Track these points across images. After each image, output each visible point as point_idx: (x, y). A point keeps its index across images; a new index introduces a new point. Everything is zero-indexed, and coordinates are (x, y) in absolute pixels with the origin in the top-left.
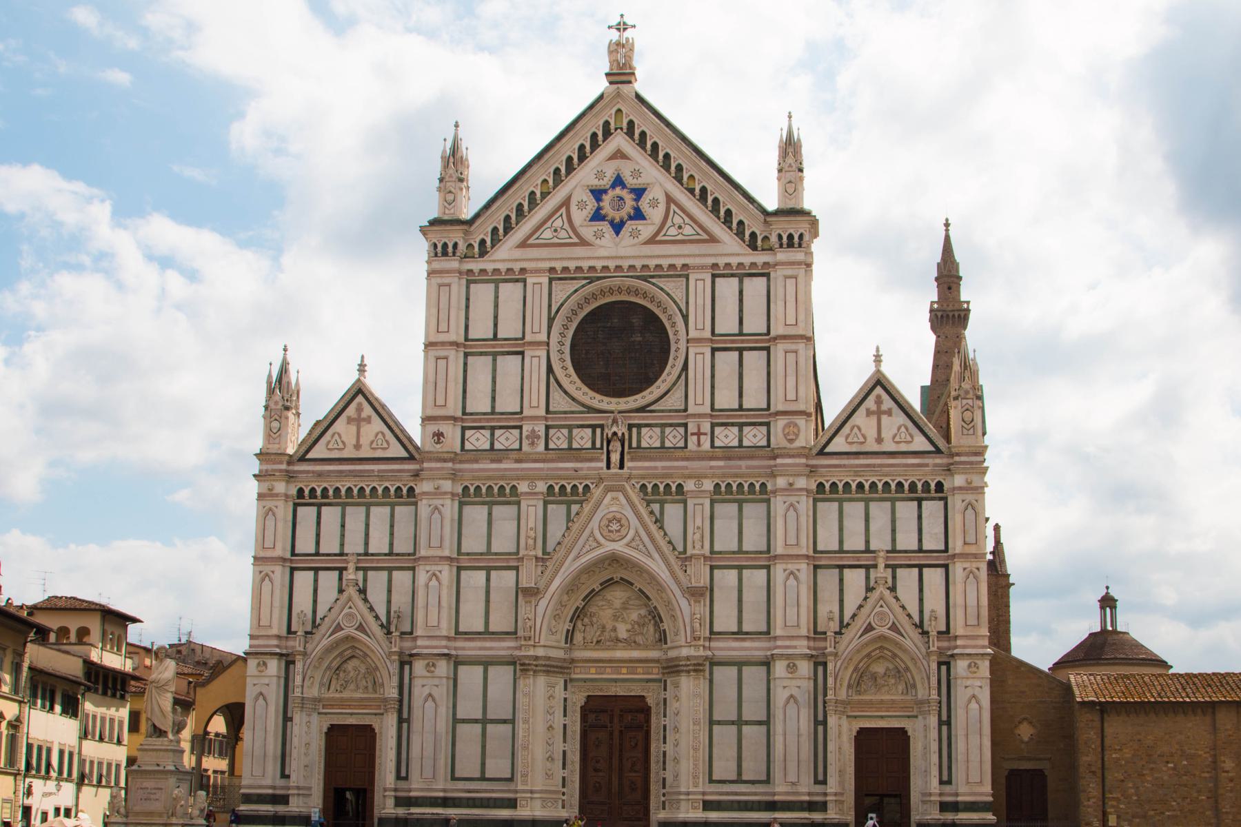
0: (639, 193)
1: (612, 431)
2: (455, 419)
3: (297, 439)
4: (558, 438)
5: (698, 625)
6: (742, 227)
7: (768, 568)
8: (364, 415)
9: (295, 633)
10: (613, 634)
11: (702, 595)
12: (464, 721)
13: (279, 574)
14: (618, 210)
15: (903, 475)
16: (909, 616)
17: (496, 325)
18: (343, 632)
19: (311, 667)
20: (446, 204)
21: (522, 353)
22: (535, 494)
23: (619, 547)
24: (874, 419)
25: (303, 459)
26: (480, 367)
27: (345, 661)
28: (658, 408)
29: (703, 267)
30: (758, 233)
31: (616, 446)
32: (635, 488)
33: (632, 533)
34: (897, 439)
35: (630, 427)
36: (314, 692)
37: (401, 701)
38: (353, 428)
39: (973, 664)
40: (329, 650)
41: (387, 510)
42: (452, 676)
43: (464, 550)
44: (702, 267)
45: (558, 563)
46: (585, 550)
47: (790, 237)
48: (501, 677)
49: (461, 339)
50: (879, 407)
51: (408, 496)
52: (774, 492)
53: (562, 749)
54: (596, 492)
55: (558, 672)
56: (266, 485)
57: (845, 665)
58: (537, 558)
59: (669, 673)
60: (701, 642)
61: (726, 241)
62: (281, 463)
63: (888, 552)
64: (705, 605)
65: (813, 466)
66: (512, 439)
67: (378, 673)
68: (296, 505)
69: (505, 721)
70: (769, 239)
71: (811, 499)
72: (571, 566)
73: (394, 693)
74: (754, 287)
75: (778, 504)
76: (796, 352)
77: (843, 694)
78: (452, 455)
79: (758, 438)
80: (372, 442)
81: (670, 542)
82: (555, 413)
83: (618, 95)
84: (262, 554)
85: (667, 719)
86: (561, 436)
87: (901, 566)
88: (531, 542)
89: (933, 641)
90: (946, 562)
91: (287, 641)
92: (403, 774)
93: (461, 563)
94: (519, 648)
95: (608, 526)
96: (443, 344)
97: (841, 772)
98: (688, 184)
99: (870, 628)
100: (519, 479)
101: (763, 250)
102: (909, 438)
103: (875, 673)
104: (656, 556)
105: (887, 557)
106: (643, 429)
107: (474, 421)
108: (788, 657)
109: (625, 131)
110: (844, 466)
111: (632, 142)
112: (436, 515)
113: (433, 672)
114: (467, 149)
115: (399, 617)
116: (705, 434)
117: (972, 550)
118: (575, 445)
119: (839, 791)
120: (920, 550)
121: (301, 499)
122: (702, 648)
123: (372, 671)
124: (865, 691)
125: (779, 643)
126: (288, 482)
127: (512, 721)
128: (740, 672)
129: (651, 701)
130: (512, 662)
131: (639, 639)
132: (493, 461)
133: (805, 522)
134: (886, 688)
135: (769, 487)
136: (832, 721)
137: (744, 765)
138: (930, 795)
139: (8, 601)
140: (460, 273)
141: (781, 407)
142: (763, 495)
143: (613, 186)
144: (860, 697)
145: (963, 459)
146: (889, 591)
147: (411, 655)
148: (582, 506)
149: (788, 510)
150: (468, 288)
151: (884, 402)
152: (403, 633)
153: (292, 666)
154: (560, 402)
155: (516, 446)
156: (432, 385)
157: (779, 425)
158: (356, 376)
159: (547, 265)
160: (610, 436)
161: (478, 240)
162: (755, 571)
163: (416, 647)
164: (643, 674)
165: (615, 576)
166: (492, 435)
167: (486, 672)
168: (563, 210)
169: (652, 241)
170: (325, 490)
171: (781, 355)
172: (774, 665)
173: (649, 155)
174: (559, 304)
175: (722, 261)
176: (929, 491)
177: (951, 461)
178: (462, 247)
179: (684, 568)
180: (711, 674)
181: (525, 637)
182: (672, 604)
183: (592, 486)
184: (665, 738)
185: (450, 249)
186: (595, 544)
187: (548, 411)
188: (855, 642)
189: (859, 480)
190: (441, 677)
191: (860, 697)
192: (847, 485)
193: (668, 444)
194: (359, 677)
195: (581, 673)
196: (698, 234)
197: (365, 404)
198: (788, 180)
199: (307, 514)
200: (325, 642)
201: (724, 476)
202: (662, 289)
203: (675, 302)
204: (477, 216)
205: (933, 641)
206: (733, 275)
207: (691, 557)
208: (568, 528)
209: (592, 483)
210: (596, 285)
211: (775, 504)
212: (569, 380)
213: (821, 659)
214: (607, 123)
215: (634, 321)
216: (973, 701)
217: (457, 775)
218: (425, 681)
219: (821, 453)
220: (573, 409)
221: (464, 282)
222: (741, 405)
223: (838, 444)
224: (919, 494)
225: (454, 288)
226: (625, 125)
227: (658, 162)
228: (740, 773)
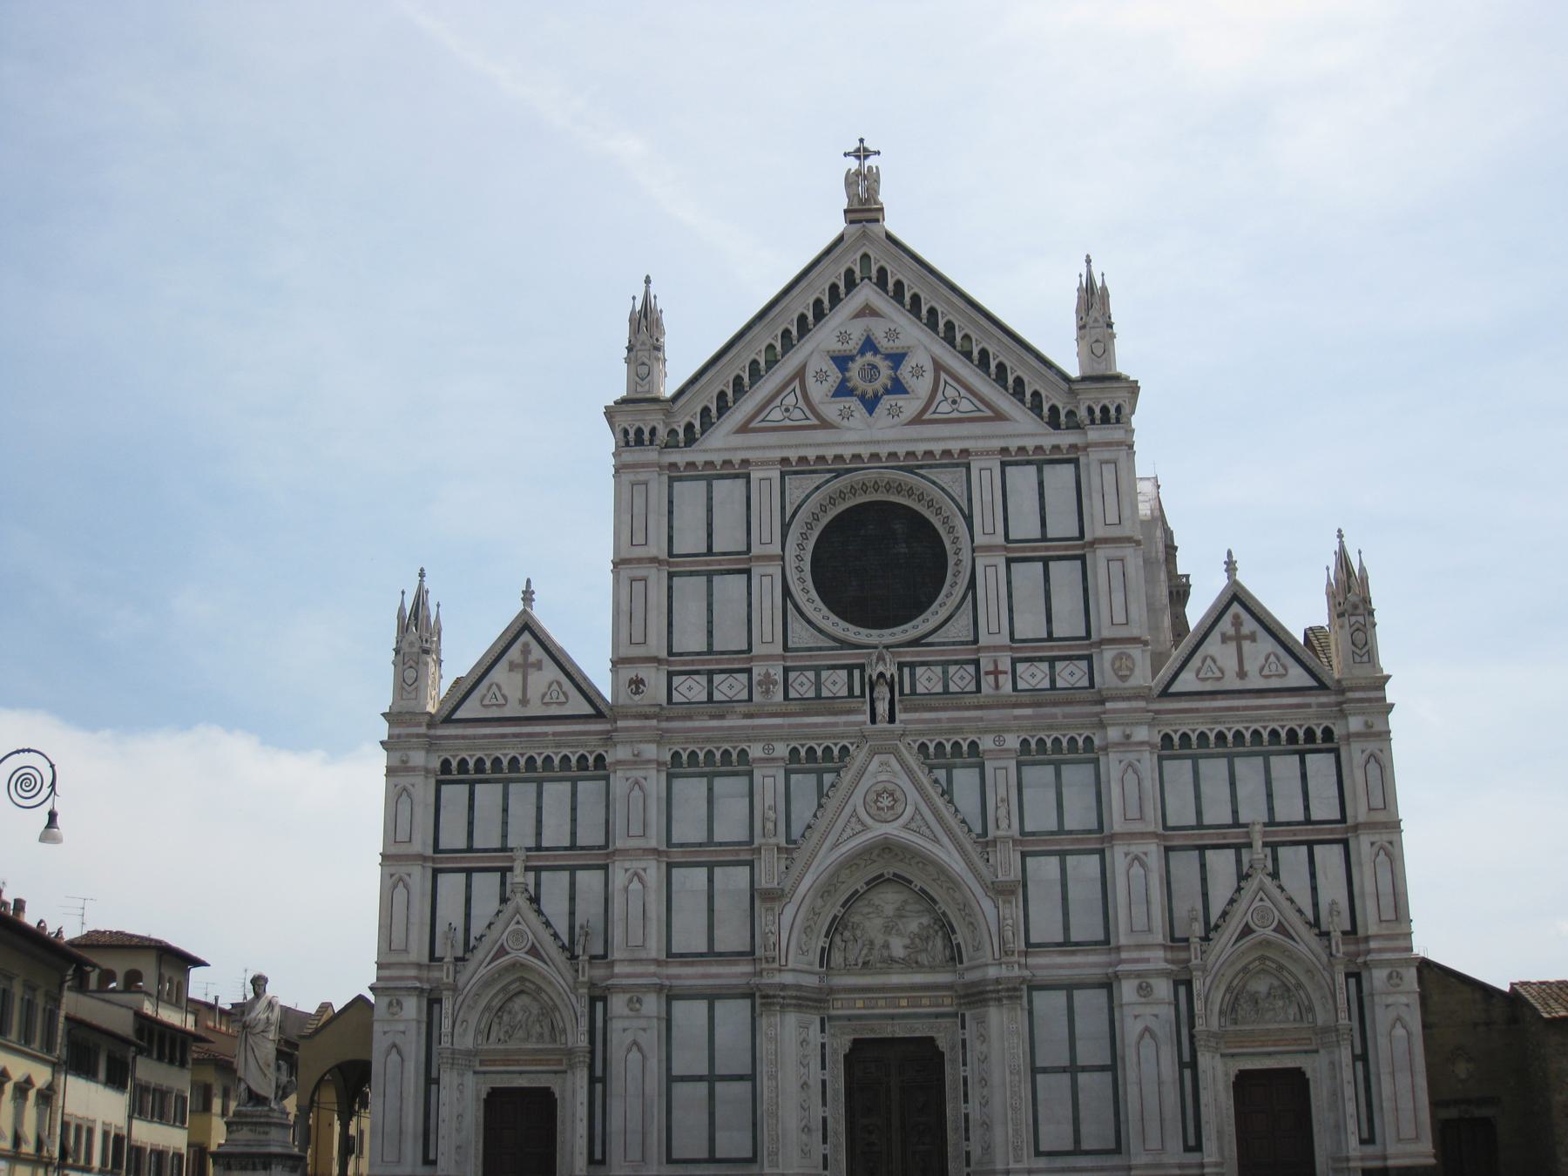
0: (897, 359)
1: (878, 671)
2: (657, 660)
3: (439, 694)
4: (802, 684)
5: (1011, 933)
9: (441, 959)
10: (886, 954)
11: (1013, 892)
12: (683, 1079)
13: (418, 877)
14: (870, 382)
15: (1278, 720)
16: (1300, 911)
17: (710, 536)
18: (507, 957)
19: (465, 1005)
21: (748, 572)
22: (773, 759)
23: (893, 830)
24: (1232, 646)
25: (448, 720)
26: (690, 590)
27: (510, 999)
28: (937, 640)
29: (988, 453)
30: (1060, 406)
31: (883, 691)
32: (911, 748)
34: (1266, 672)
36: (467, 1042)
37: (592, 1052)
39: (1395, 974)
40: (487, 983)
41: (567, 786)
42: (664, 1014)
43: (675, 840)
44: (987, 453)
46: (845, 836)
47: (1105, 410)
48: (733, 1014)
49: (664, 555)
50: (1238, 631)
51: (596, 768)
52: (1105, 749)
53: (820, 1114)
54: (859, 756)
55: (812, 1007)
56: (398, 754)
58: (779, 849)
59: (969, 1003)
60: (1015, 958)
61: (1018, 419)
62: (419, 725)
63: (1265, 825)
64: (1017, 907)
66: (738, 687)
67: (557, 1014)
68: (439, 783)
69: (740, 1078)
70: (1076, 416)
71: (1156, 756)
72: (826, 860)
73: (583, 1041)
74: (1060, 478)
75: (1113, 765)
76: (1122, 560)
78: (657, 709)
80: (544, 696)
82: (797, 650)
84: (394, 850)
85: (968, 1068)
86: (805, 680)
87: (1284, 844)
88: (770, 826)
90: (1345, 836)
91: (429, 971)
92: (598, 1156)
93: (673, 857)
96: (639, 561)
97: (1220, 1134)
98: (962, 346)
99: (1247, 931)
100: (749, 741)
101: (1067, 428)
102: (1281, 671)
103: (1256, 992)
104: (945, 840)
106: (917, 669)
107: (685, 663)
108: (1139, 975)
109: (874, 280)
110: (1197, 710)
111: (885, 295)
112: (637, 792)
113: (638, 1010)
115: (587, 934)
116: (1006, 673)
117: (1380, 817)
118: (825, 693)
120: (1308, 821)
121: (446, 773)
122: (1016, 966)
123: (548, 1012)
126: (428, 751)
127: (752, 1077)
128: (1070, 999)
129: (943, 1045)
131: (923, 958)
132: (712, 717)
133: (1151, 786)
135: (1097, 742)
136: (1204, 1060)
137: (1084, 1129)
138: (1348, 1159)
139: (39, 924)
141: (1106, 634)
142: (1090, 753)
143: (862, 352)
144: (1238, 1028)
145: (1358, 695)
146: (1270, 879)
147: (608, 988)
149: (1125, 771)
150: (670, 487)
151: (1244, 623)
152: (593, 957)
153: (436, 1007)
154: (801, 635)
156: (625, 616)
158: (520, 606)
159: (778, 454)
160: (874, 677)
161: (683, 425)
162: (1084, 858)
163: (612, 976)
164: (930, 1006)
165: (885, 872)
166: (710, 681)
168: (797, 383)
169: (918, 420)
170: (480, 762)
171: (1102, 564)
172: (1120, 987)
173: (908, 311)
174: (795, 506)
175: (1013, 444)
177: (1340, 699)
178: (662, 433)
179: (986, 856)
180: (1030, 1002)
181: (766, 958)
184: (966, 1095)
185: (646, 436)
186: (859, 827)
187: (786, 648)
188: (1229, 950)
189: (1218, 728)
190: (649, 1017)
191: (1238, 1028)
192: (1203, 736)
193: (953, 688)
194: (531, 1019)
195: (842, 1008)
196: (979, 410)
197: (534, 644)
199: (455, 795)
200: (482, 971)
202: (934, 483)
203: (953, 499)
204: (681, 392)
206: (1029, 463)
208: (820, 806)
209: (852, 744)
210: (845, 480)
211: (1108, 764)
212: (813, 606)
213: (1184, 977)
215: (897, 527)
216: (1398, 1025)
217: (675, 1155)
218: (626, 1024)
219: (1165, 693)
220: (820, 644)
221: (665, 479)
222: (1050, 633)
223: (1187, 682)
224: (1302, 743)
225: (653, 486)
227: (920, 319)
228: (1077, 1139)
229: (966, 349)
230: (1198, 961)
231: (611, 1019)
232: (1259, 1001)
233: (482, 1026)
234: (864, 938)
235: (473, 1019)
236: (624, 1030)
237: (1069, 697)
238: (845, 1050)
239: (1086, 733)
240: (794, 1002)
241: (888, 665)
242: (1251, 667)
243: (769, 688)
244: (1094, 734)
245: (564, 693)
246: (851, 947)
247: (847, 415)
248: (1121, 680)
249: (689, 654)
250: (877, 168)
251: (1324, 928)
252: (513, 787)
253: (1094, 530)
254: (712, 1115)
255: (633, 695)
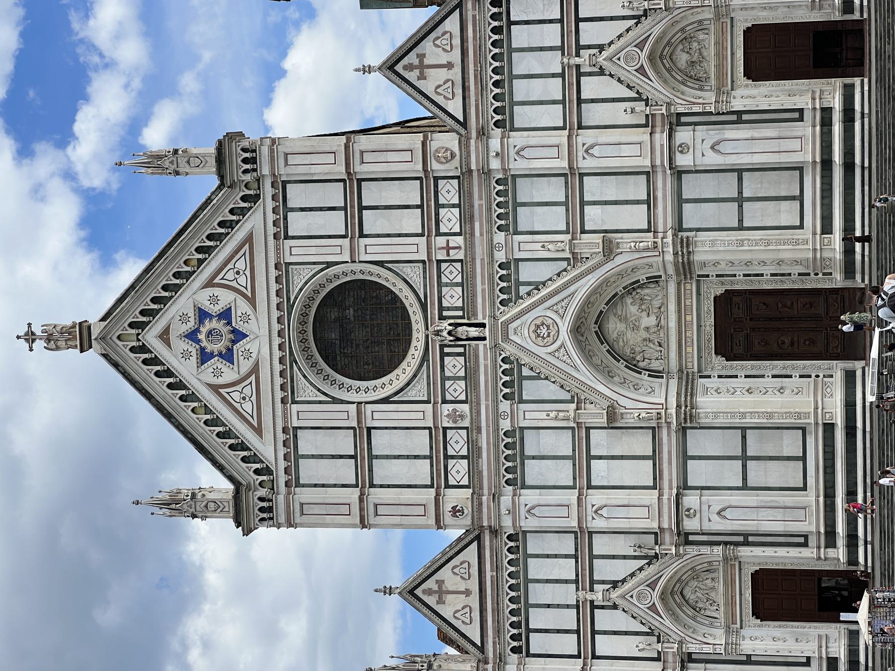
0: (202, 315)
1: (447, 335)
4: (455, 390)
5: (641, 244)
6: (236, 211)
7: (582, 175)
8: (436, 588)
9: (659, 653)
12: (745, 479)
16: (628, 30)
17: (341, 457)
20: (219, 510)
21: (369, 429)
23: (565, 326)
25: (482, 649)
27: (687, 601)
29: (277, 249)
30: (242, 194)
33: (549, 313)
35: (441, 318)
38: (449, 598)
40: (676, 618)
45: (582, 388)
46: (569, 361)
48: (698, 442)
52: (505, 170)
54: (509, 350)
55: (692, 385)
57: (679, 94)
60: (659, 241)
63: (563, 54)
65: (478, 132)
67: (697, 568)
68: (528, 655)
69: (744, 438)
72: (585, 375)
73: (718, 550)
74: (297, 196)
75: (518, 166)
77: (711, 97)
79: (451, 189)
81: (558, 275)
83: (103, 338)
86: (452, 388)
89: (654, 4)
91: (667, 662)
92: (802, 540)
94: (669, 424)
95: (543, 337)
96: (361, 509)
99: (641, 70)
100: (498, 429)
101: (259, 189)
104: (572, 289)
105: (568, 55)
107: (439, 475)
114: (160, 492)
116: (448, 240)
118: (462, 373)
119: (810, 95)
122: (665, 240)
123: (695, 574)
124: (706, 73)
125: (658, 162)
127: (744, 430)
128: (688, 201)
129: (720, 291)
130: (683, 431)
131: (656, 303)
132: (479, 456)
134: (703, 50)
135: (500, 176)
137: (783, 194)
140: (289, 493)
141: (420, 167)
142: (509, 181)
146: (603, 52)
147: (679, 534)
148: (524, 365)
149: (523, 157)
150: (304, 486)
151: (411, 62)
152: (656, 543)
153: (694, 656)
154: (419, 391)
155: (464, 433)
157: (436, 167)
159: (279, 405)
160: (452, 338)
161: (256, 477)
165: (593, 330)
166: (453, 457)
167: (694, 458)
168: (222, 391)
172: (681, 166)
174: (318, 393)
175: (271, 230)
176: (500, 14)
179: (584, 260)
180: (690, 230)
182: (620, 271)
183: (504, 355)
185: (265, 504)
186: (562, 350)
187: (428, 402)
188: (656, 85)
189: (490, 85)
195: (692, 362)
196: (244, 254)
197: (424, 586)
198: (187, 165)
199: (537, 643)
200: (667, 622)
201: (490, 221)
202: (301, 290)
203: (314, 276)
204: (231, 478)
205: (654, 4)
206: (285, 218)
207: (573, 253)
208: (546, 378)
209: (500, 355)
210: (298, 356)
213: (674, 120)
214: (133, 350)
219: (464, 124)
222: (417, 207)
223: (455, 107)
226: (134, 331)
228: (793, 198)
229: (195, 263)
230: (664, 108)
231: (701, 530)
232: (693, 60)
233: (707, 622)
234: (641, 345)
235: (703, 629)
236: (710, 520)
237: (465, 193)
238: (723, 361)
239: (493, 183)
240: (689, 398)
241: (443, 328)
242: (444, 59)
243: (459, 415)
244: (494, 178)
245: (461, 564)
246: (649, 355)
247: (248, 354)
248: (454, 157)
249: (432, 473)
250: (42, 326)
251: (641, 13)
252: (531, 601)
253: (340, 170)
254: (771, 458)
255: (464, 515)
